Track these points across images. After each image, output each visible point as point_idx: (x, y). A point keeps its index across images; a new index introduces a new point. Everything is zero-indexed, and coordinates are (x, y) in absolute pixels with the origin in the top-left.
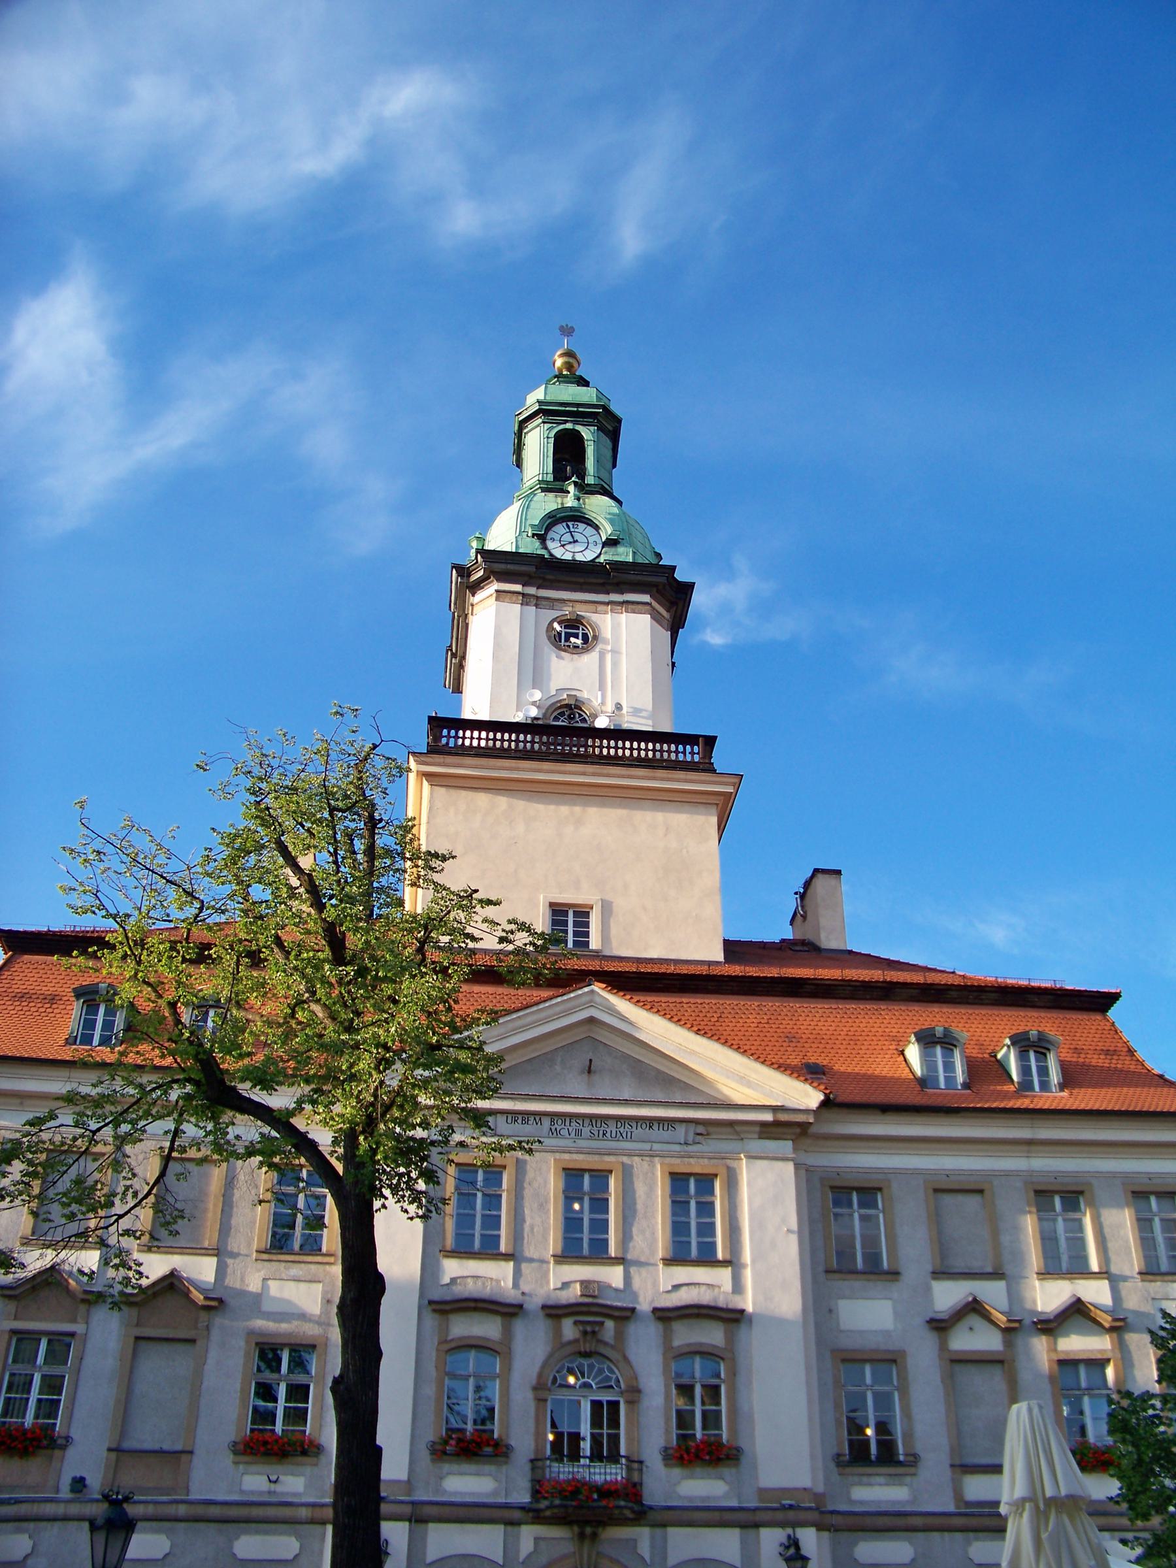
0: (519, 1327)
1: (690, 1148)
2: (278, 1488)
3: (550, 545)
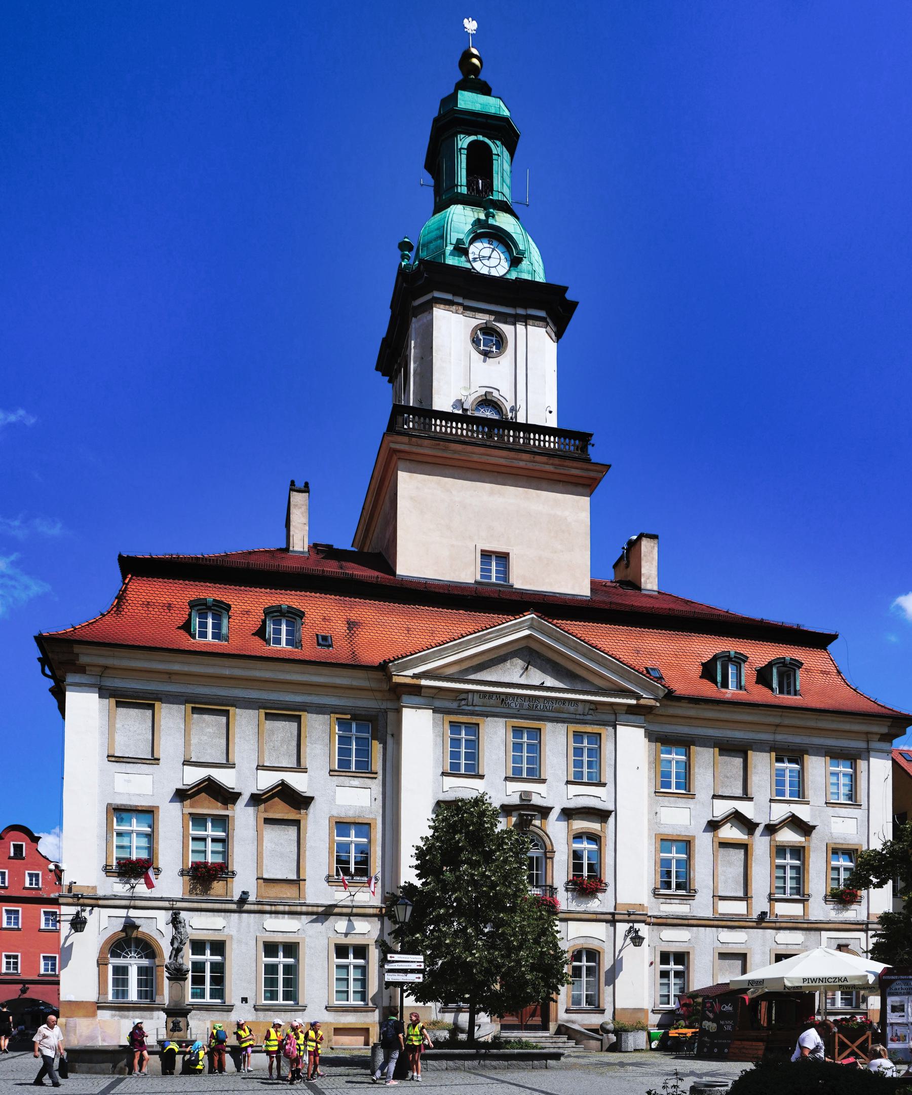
1: (585, 718)
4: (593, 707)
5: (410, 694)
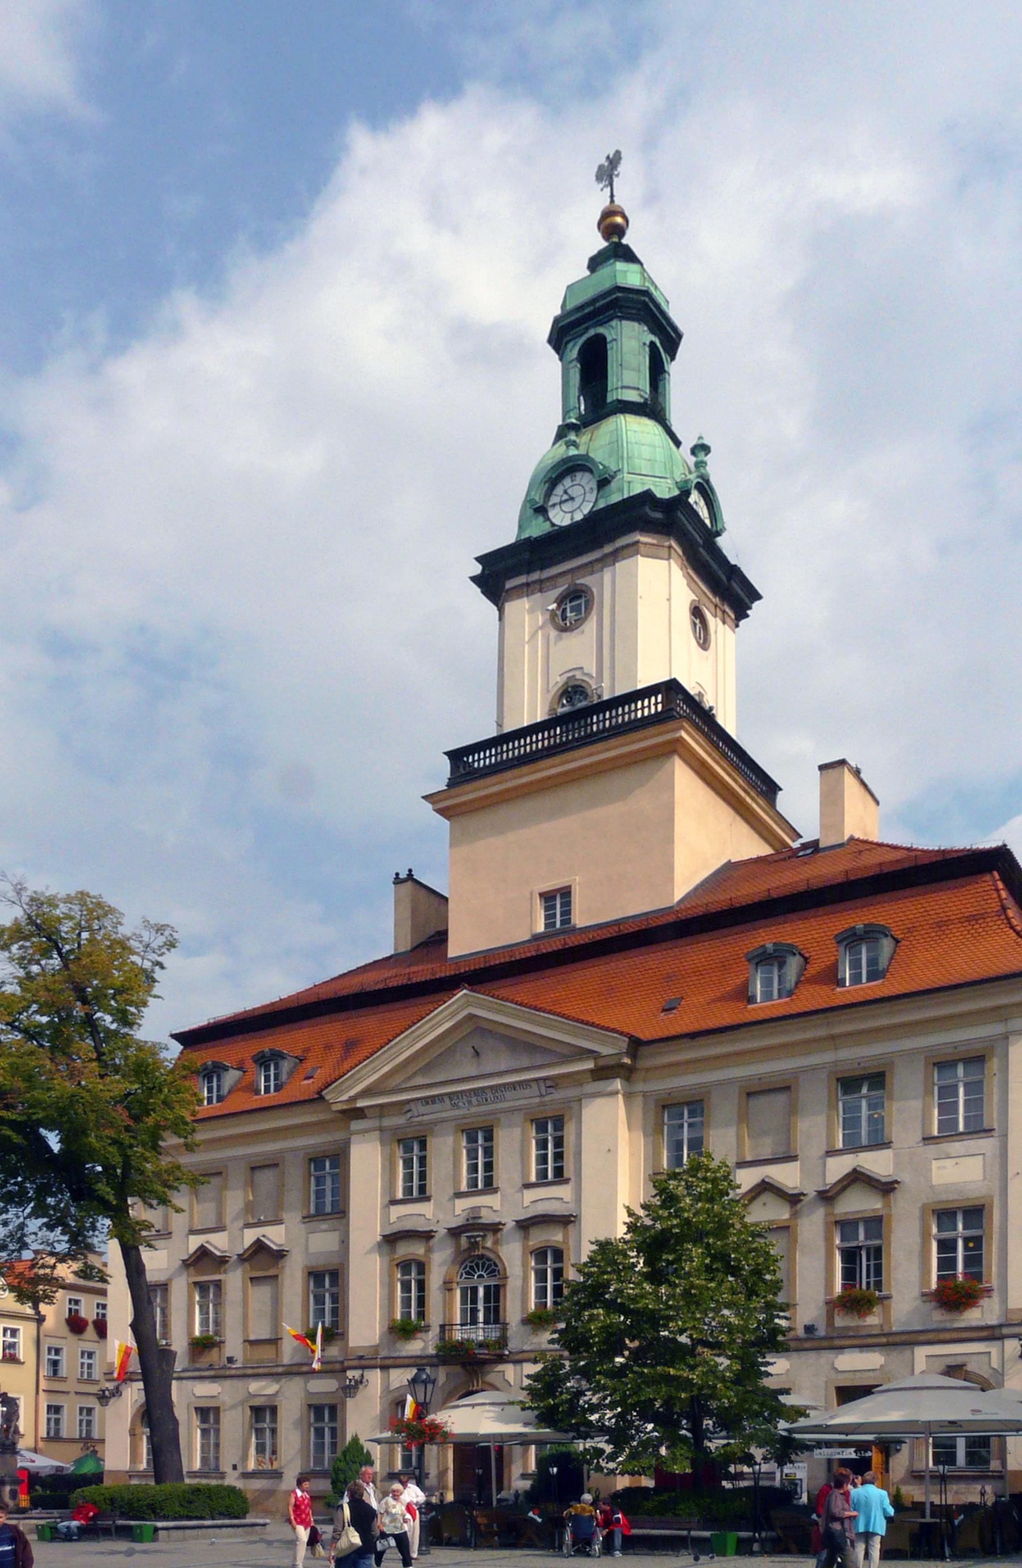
4: (549, 1083)
5: (357, 1118)
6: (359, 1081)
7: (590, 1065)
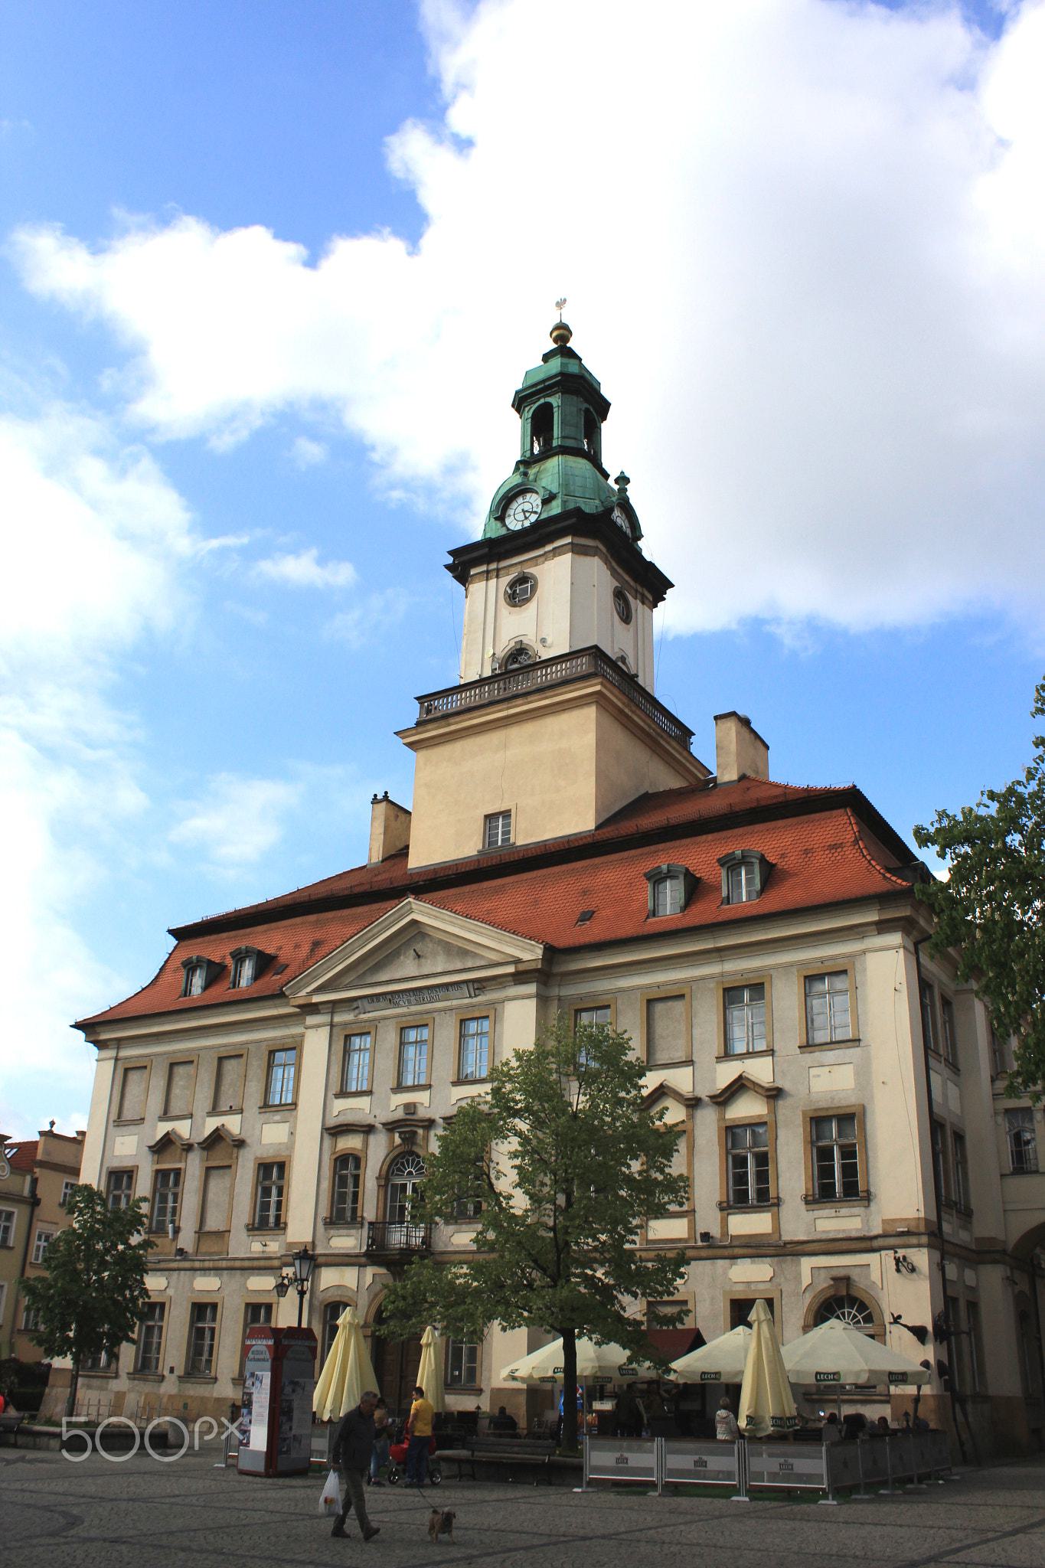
0: (372, 1138)
2: (267, 1249)
3: (507, 521)
6: (316, 978)
7: (511, 969)
